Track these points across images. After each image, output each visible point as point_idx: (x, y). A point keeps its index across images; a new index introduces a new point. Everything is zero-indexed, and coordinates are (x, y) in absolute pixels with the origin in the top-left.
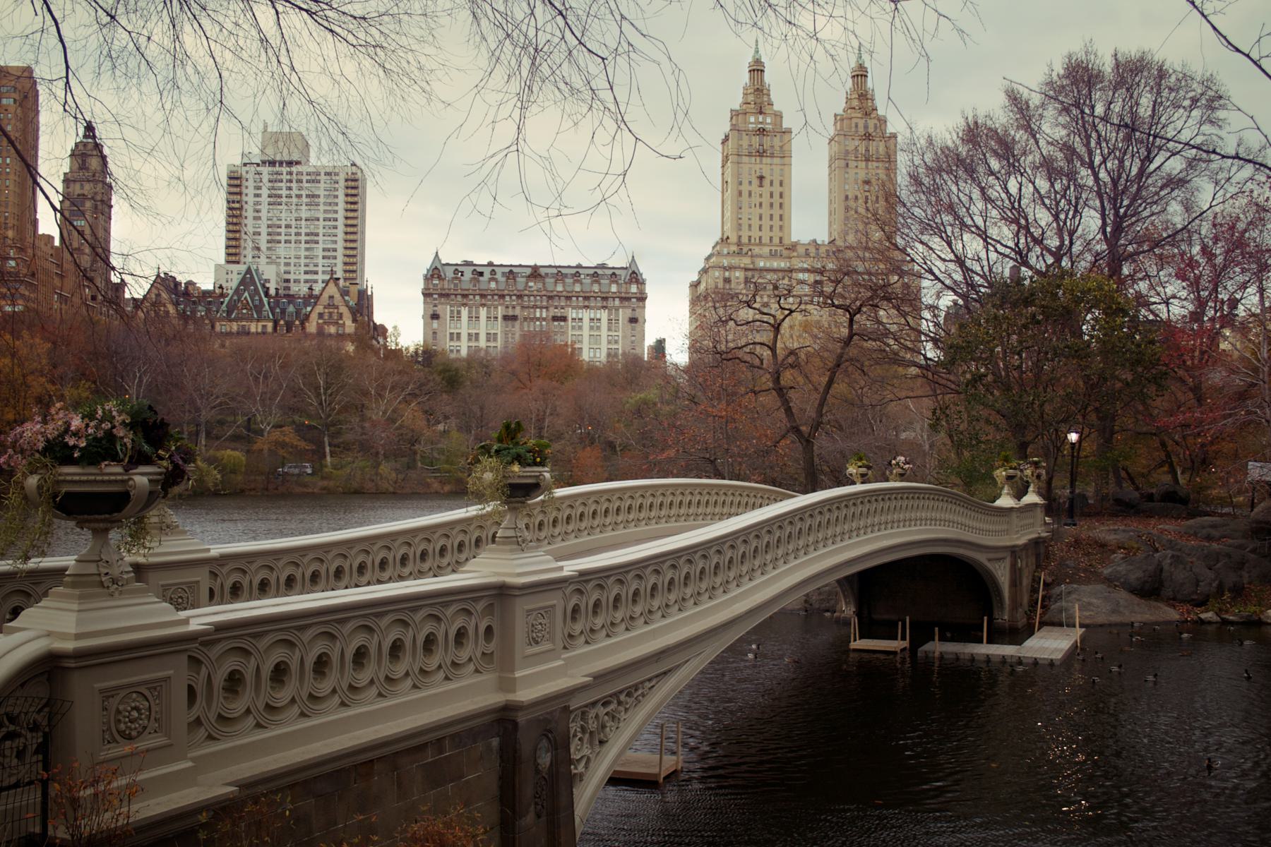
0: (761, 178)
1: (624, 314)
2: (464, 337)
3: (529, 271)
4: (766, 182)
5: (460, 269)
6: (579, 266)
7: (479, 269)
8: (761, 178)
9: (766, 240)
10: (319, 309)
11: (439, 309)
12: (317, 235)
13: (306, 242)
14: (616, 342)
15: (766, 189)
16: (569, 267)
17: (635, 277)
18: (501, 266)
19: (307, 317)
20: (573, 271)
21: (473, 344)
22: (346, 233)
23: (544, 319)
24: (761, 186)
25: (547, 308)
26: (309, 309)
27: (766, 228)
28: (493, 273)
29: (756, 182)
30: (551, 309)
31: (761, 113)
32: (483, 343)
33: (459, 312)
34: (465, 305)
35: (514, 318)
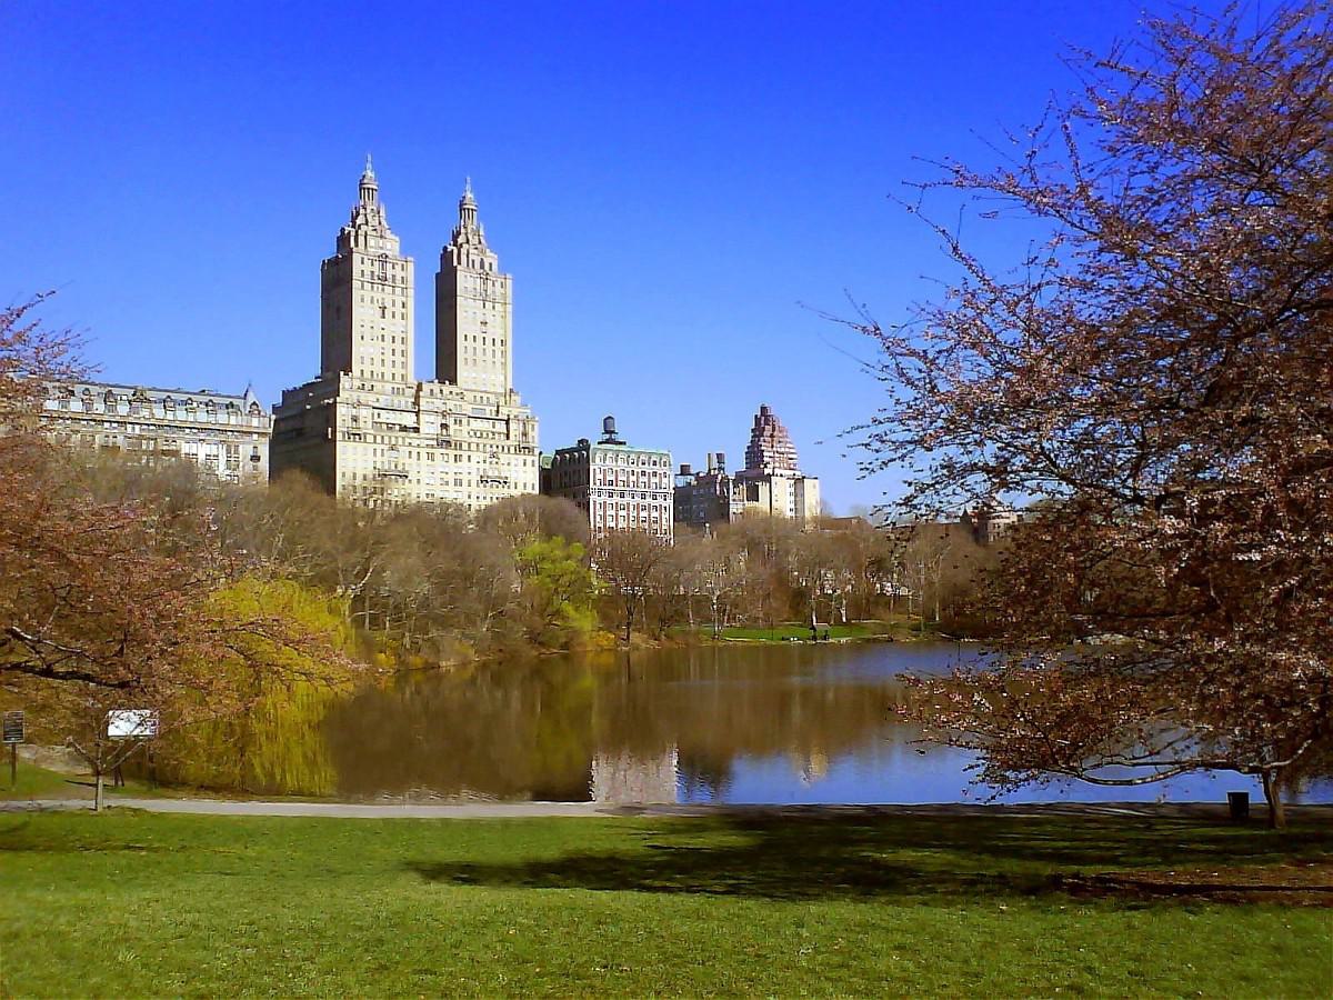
9: (388, 377)
27: (388, 363)
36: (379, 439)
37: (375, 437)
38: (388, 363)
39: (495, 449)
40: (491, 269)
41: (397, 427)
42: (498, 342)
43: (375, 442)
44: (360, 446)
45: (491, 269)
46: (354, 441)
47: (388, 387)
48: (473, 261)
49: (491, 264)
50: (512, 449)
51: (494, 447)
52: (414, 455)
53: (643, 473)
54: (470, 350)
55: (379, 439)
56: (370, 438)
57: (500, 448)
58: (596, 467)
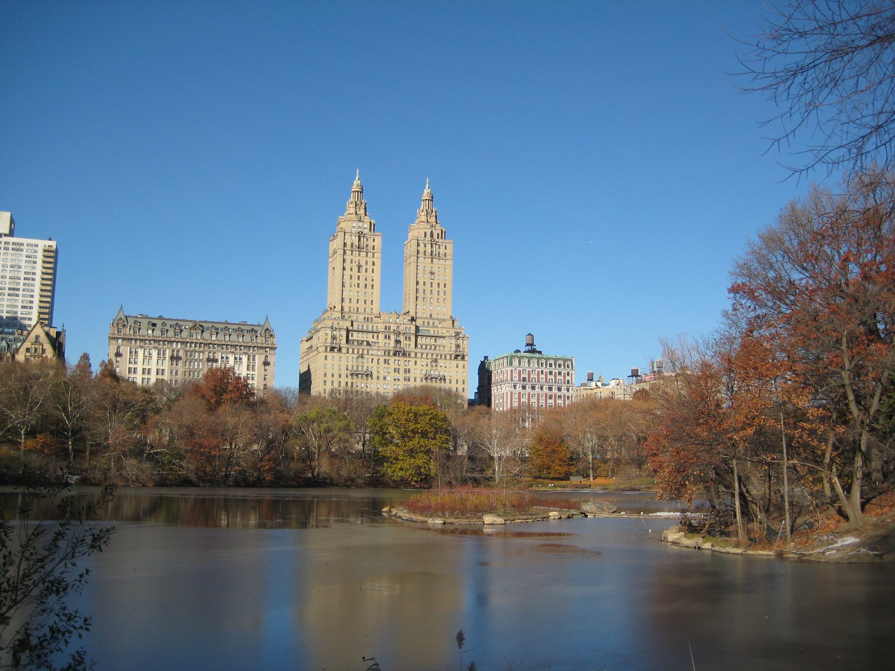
1: (259, 359)
2: (154, 372)
3: (191, 325)
4: (363, 270)
5: (139, 320)
6: (226, 323)
7: (154, 321)
8: (359, 267)
9: (361, 310)
10: (27, 344)
11: (121, 350)
12: (18, 290)
13: (9, 295)
15: (363, 274)
16: (220, 323)
17: (268, 333)
18: (170, 319)
19: (17, 350)
20: (223, 326)
21: (160, 377)
22: (42, 290)
23: (201, 360)
24: (359, 271)
25: (203, 352)
26: (19, 344)
27: (362, 302)
28: (164, 324)
29: (355, 269)
30: (206, 353)
31: (360, 221)
32: (166, 377)
33: (136, 353)
34: (141, 347)
35: (178, 358)
36: (351, 351)
38: (362, 302)
41: (365, 343)
42: (442, 286)
44: (336, 355)
47: (361, 317)
50: (448, 357)
52: (375, 361)
55: (351, 351)
56: (344, 350)
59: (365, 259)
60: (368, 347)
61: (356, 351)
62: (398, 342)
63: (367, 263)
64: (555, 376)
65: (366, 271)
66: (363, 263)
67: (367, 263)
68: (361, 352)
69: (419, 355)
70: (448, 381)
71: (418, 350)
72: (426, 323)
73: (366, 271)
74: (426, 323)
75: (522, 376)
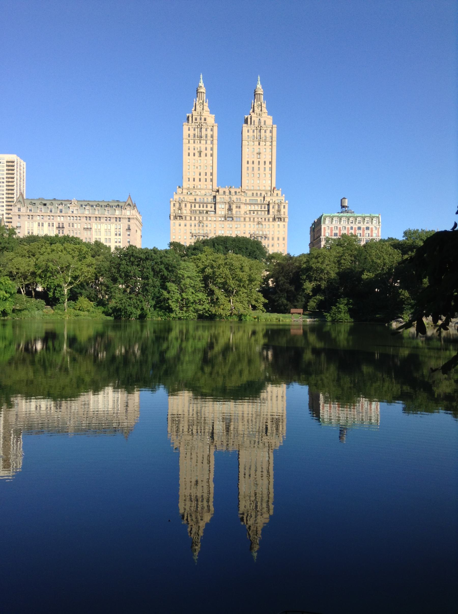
0: (200, 153)
4: (203, 154)
8: (200, 153)
14: (120, 242)
36: (193, 218)
37: (191, 217)
39: (260, 220)
40: (265, 124)
42: (268, 163)
43: (191, 219)
45: (265, 124)
46: (180, 220)
48: (254, 122)
49: (265, 122)
51: (260, 218)
53: (359, 228)
54: (250, 169)
55: (193, 218)
56: (188, 218)
57: (263, 219)
58: (326, 226)
59: (205, 146)
60: (207, 215)
61: (197, 218)
62: (230, 209)
63: (206, 149)
64: (364, 231)
65: (206, 155)
66: (203, 149)
67: (206, 149)
68: (201, 219)
69: (247, 219)
70: (271, 239)
71: (247, 216)
72: (255, 195)
73: (206, 155)
74: (255, 195)
75: (334, 232)
